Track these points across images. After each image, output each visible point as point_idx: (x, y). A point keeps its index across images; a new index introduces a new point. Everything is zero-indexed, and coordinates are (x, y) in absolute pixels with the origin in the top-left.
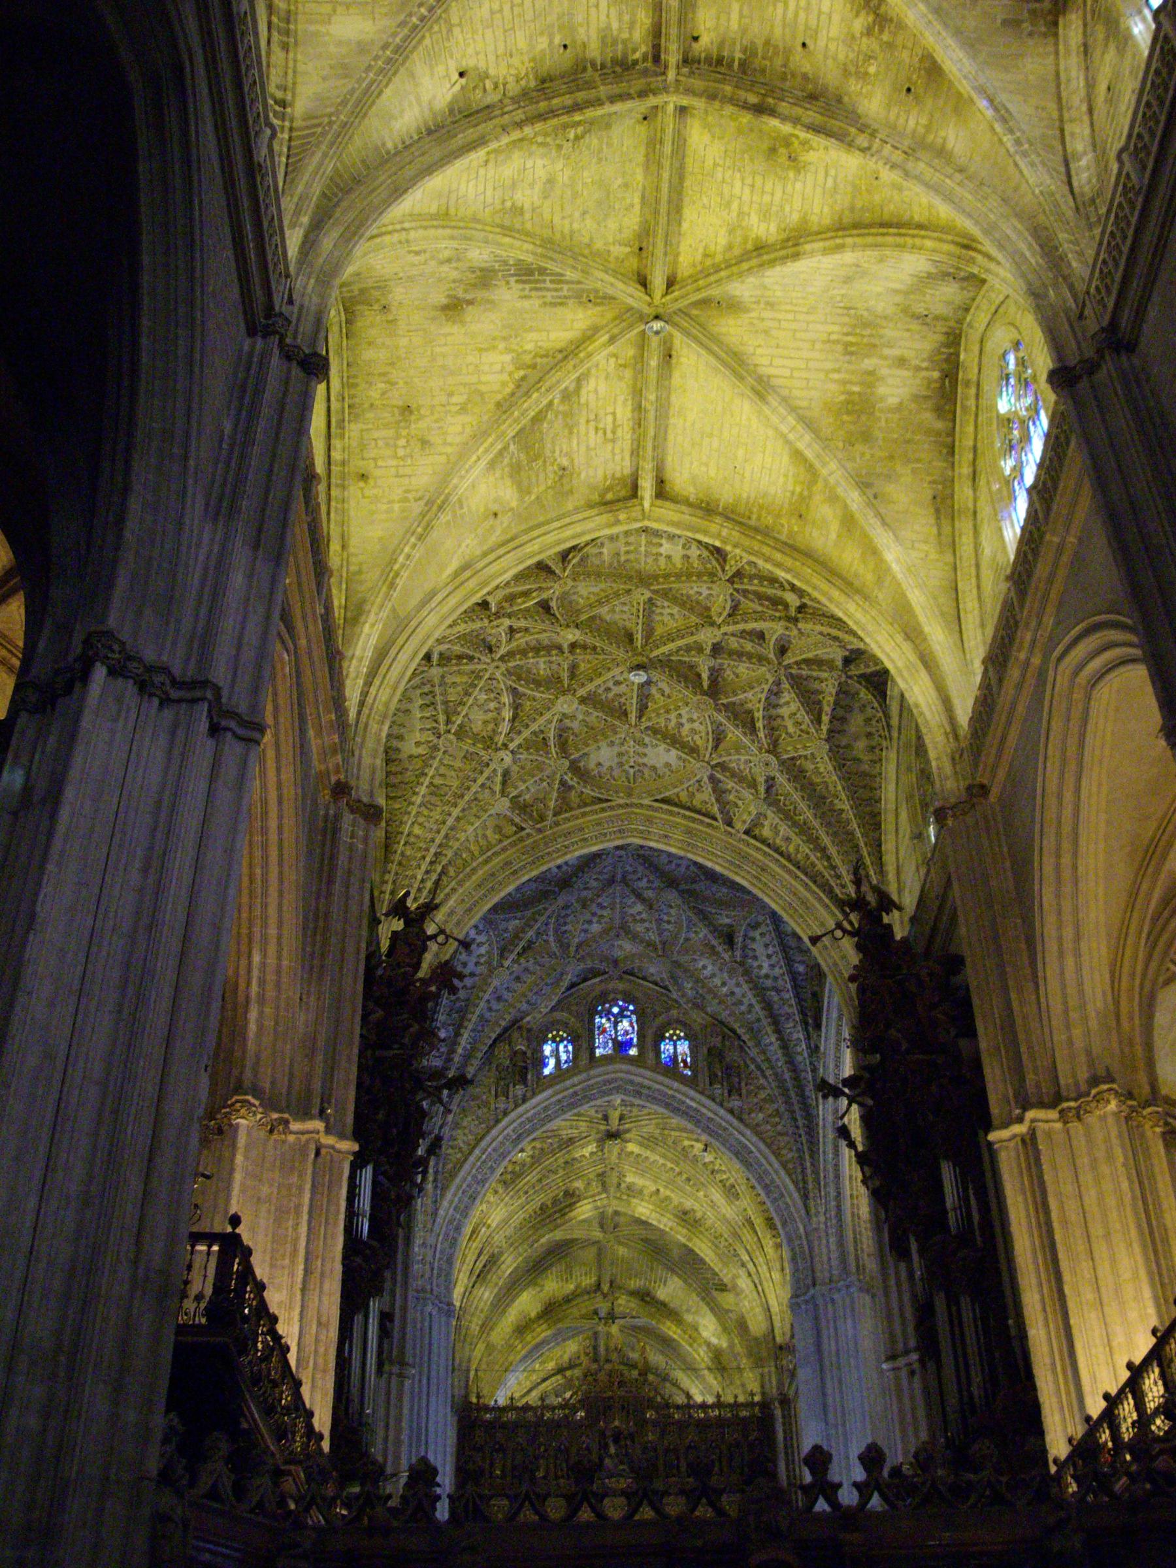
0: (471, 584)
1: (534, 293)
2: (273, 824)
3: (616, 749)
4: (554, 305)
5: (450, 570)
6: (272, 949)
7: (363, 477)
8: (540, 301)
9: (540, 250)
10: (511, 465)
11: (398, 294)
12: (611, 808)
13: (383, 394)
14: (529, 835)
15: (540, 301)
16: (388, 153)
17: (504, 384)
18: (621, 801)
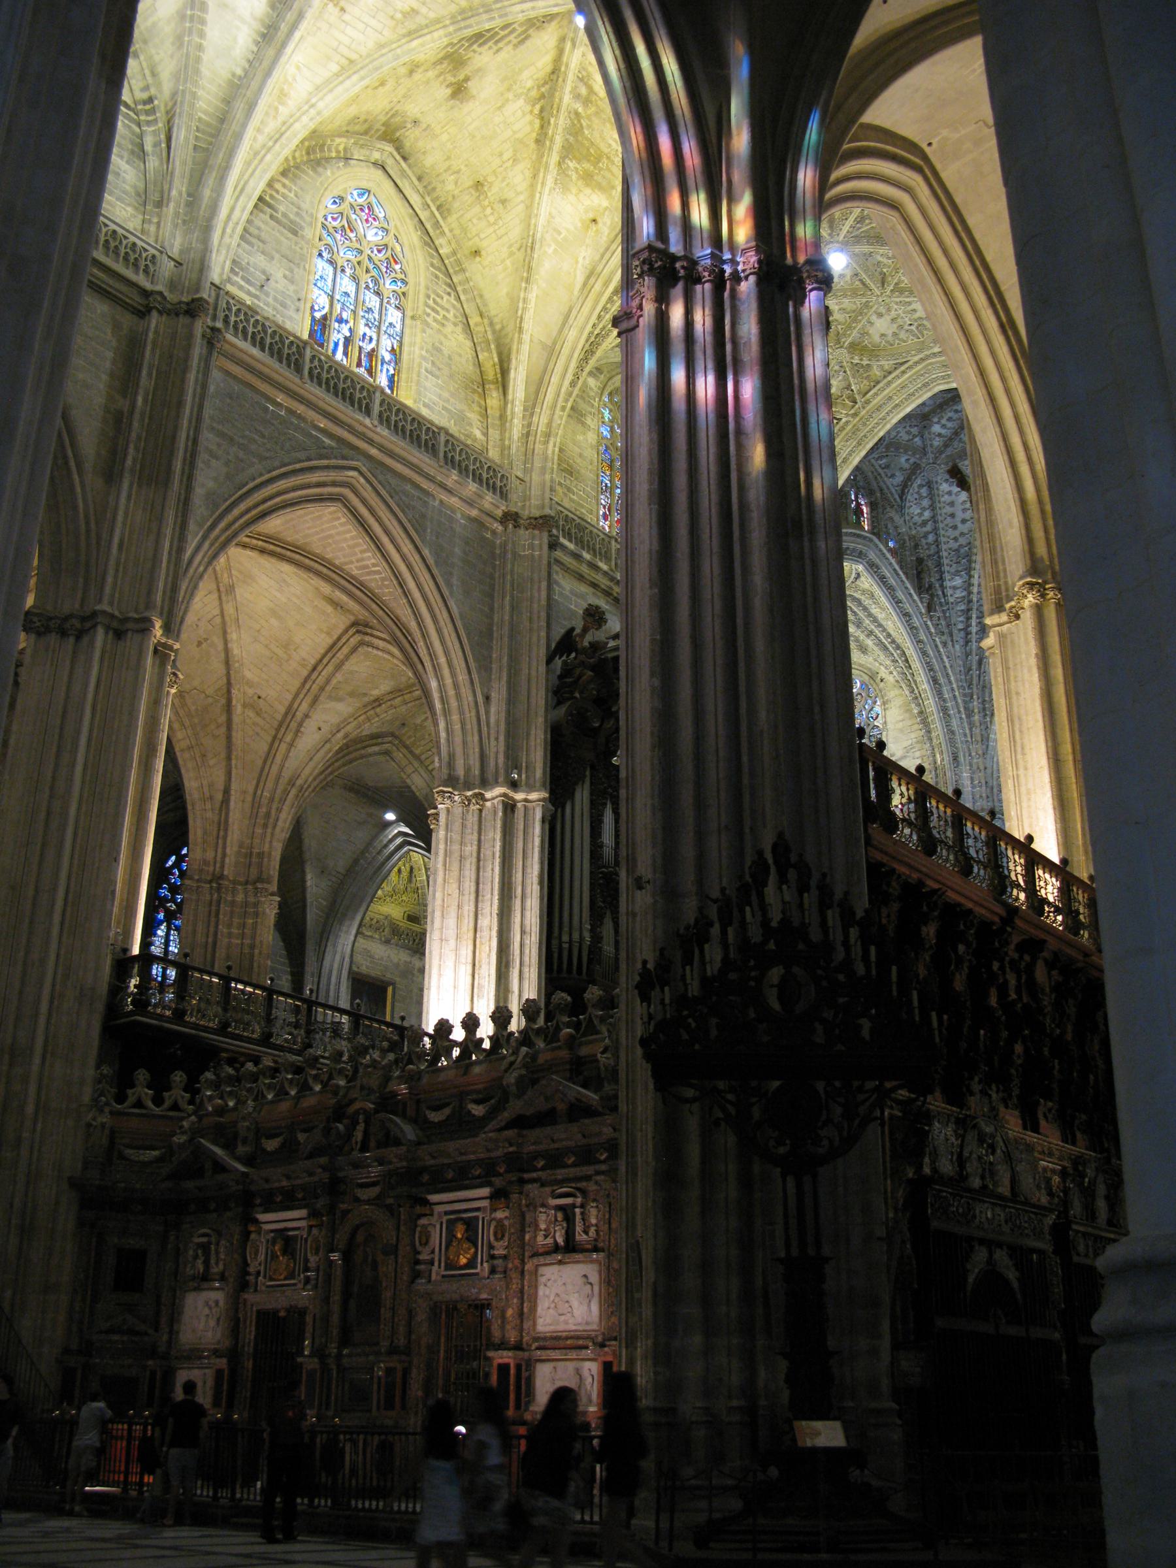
0: (598, 287)
1: (500, 45)
2: (411, 585)
3: (888, 318)
4: (522, 42)
5: (578, 286)
6: (446, 672)
7: (477, 253)
8: (510, 47)
9: (451, 29)
10: (581, 177)
11: (412, 109)
12: (910, 368)
13: (456, 183)
14: (847, 422)
15: (510, 47)
16: (240, 78)
17: (531, 123)
18: (916, 359)
